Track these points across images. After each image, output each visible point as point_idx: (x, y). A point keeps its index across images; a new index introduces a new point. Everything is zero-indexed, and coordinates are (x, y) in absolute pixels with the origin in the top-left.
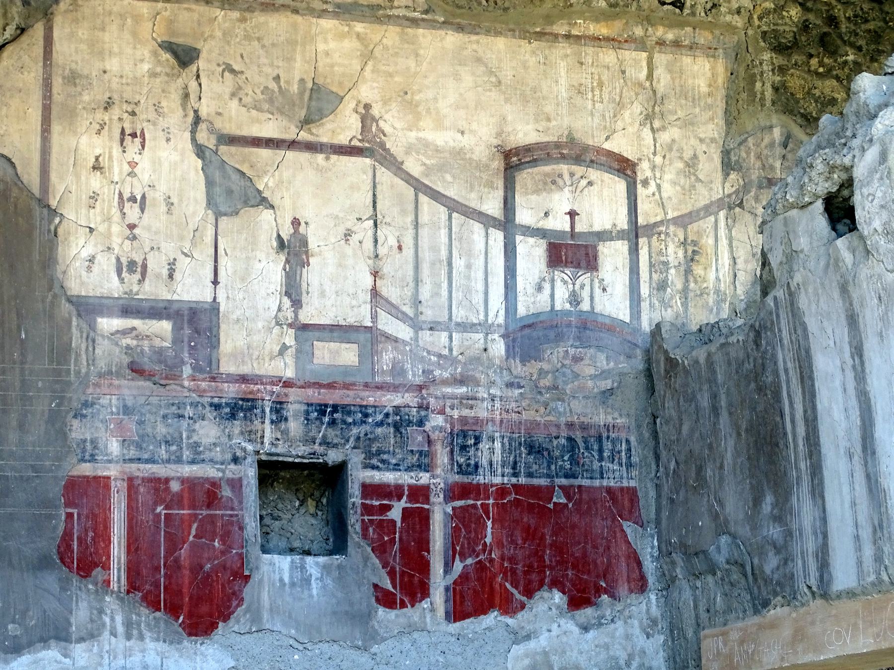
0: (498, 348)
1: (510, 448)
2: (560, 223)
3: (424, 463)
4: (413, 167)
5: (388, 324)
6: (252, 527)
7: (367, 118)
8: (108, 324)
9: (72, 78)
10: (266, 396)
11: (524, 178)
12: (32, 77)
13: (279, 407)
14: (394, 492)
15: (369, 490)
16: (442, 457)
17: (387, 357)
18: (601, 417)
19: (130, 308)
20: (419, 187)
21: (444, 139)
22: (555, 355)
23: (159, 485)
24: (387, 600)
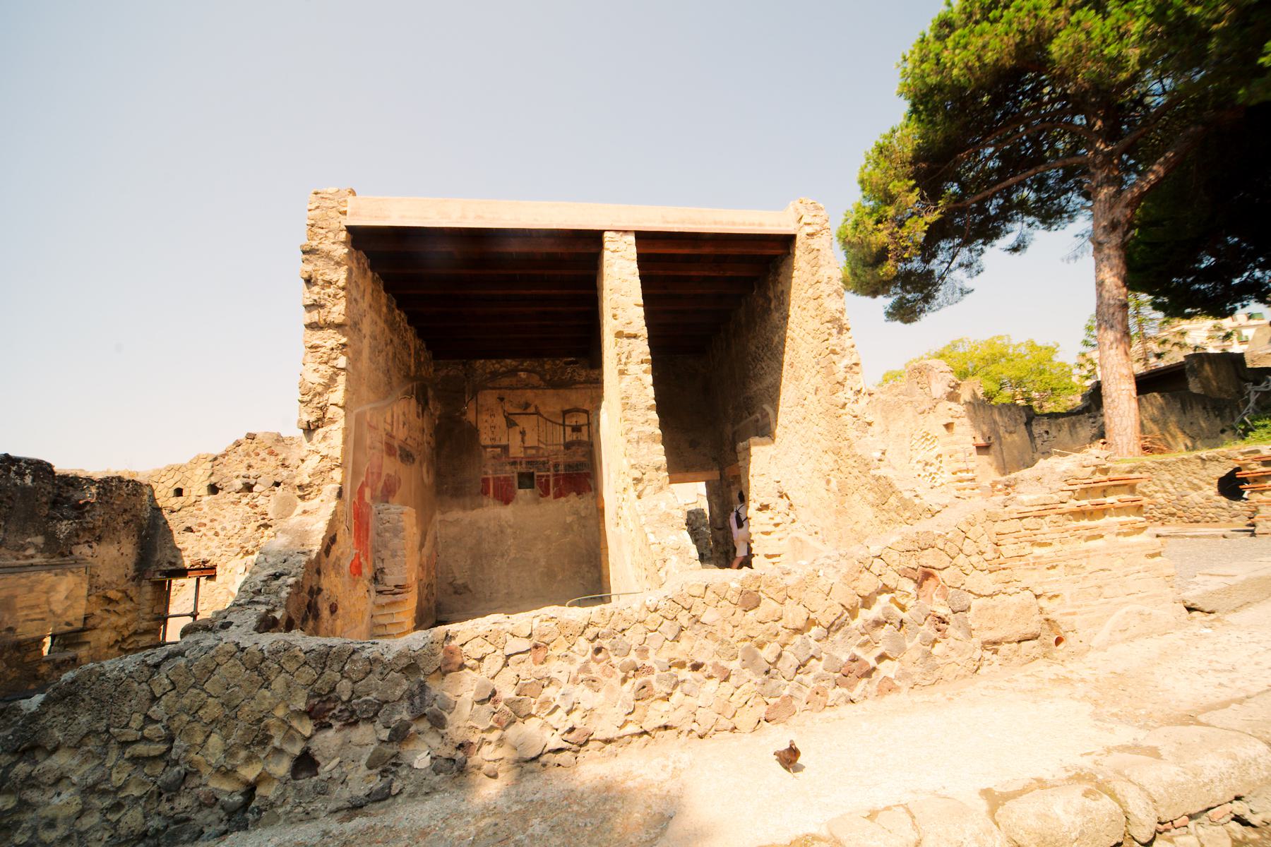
0: (562, 448)
1: (565, 467)
2: (574, 424)
3: (549, 470)
4: (545, 415)
5: (541, 445)
6: (516, 484)
7: (536, 407)
8: (489, 450)
9: (482, 406)
10: (518, 460)
11: (567, 416)
12: (474, 406)
13: (521, 463)
14: (543, 476)
15: (538, 476)
16: (552, 469)
17: (541, 451)
18: (583, 459)
19: (493, 447)
20: (546, 419)
21: (552, 410)
22: (574, 448)
23: (499, 478)
24: (542, 496)
